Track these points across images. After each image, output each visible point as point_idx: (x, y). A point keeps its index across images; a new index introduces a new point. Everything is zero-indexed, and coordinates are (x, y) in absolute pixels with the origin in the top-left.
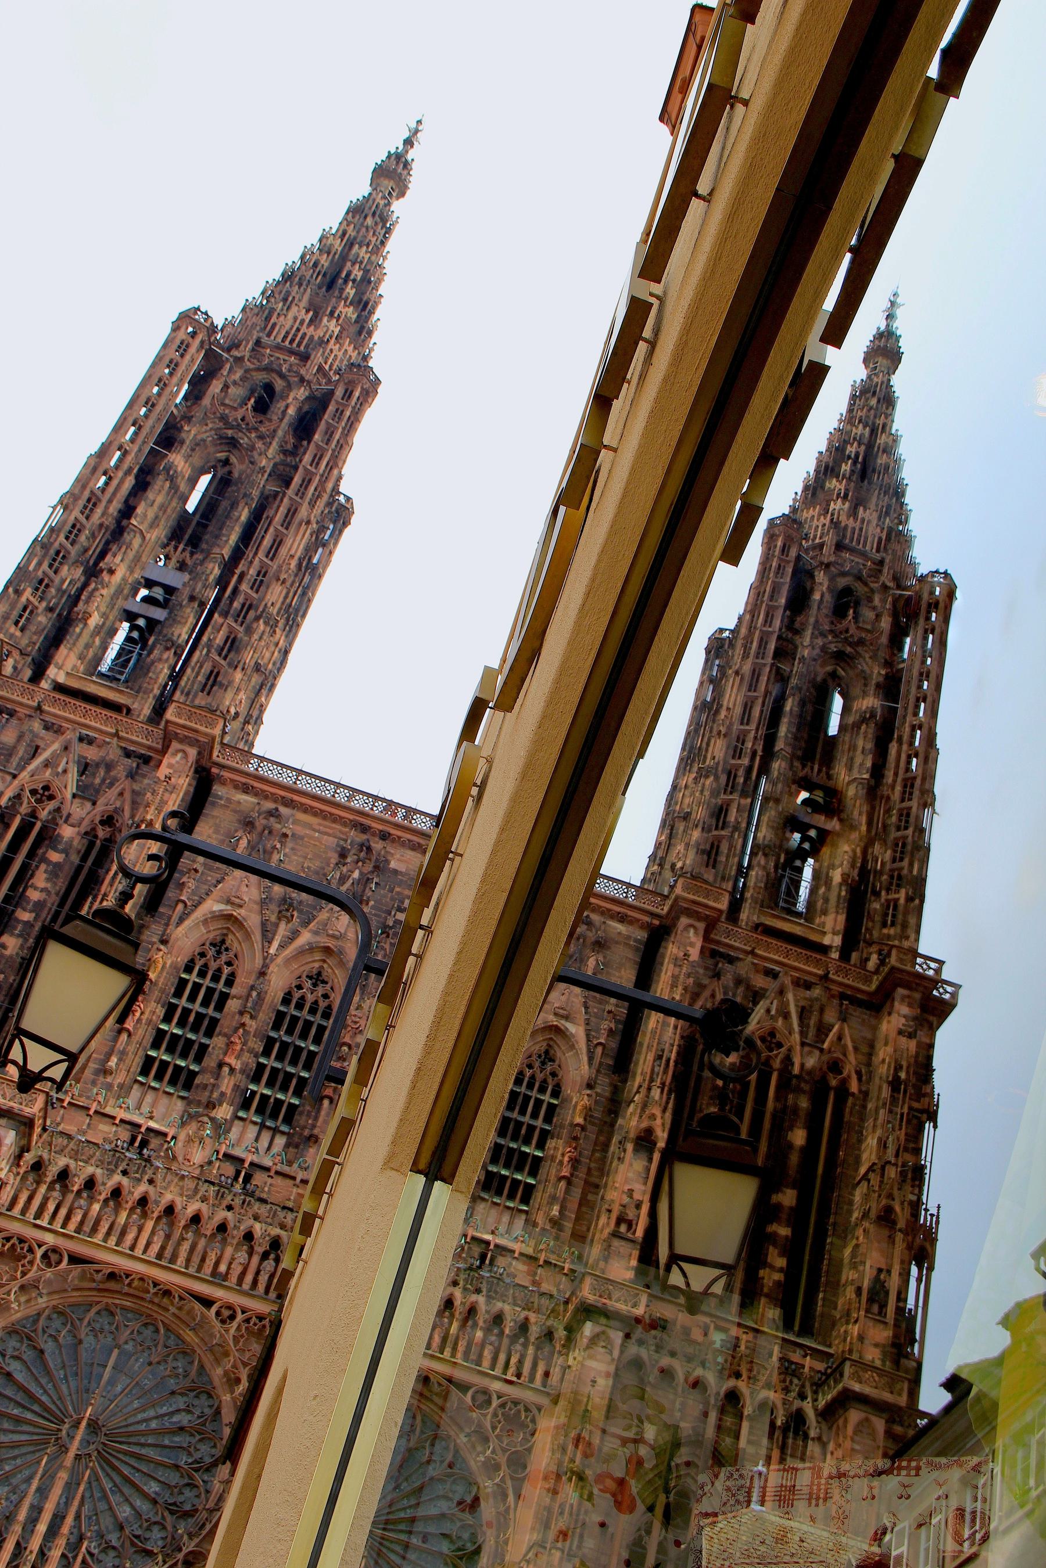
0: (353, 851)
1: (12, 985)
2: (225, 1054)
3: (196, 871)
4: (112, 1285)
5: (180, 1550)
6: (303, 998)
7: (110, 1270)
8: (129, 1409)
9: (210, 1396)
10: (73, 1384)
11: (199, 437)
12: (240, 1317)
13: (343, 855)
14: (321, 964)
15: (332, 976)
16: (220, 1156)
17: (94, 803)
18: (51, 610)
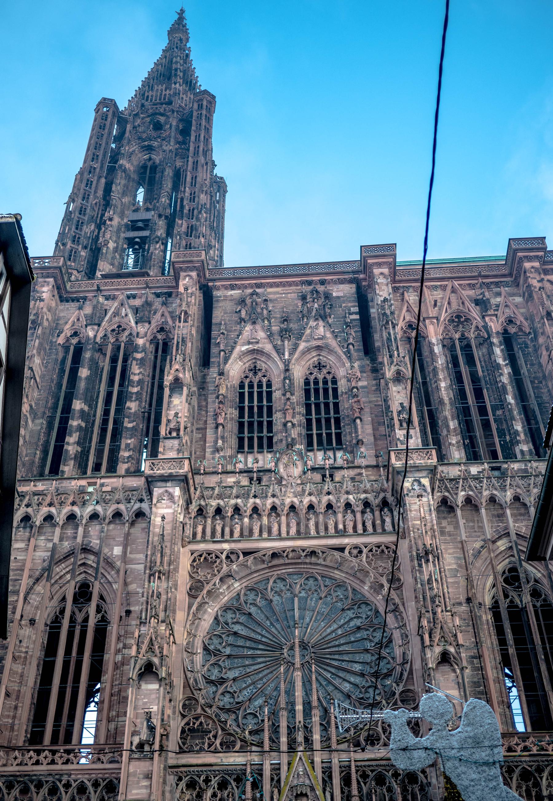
0: (308, 297)
1: (142, 429)
2: (285, 418)
3: (223, 333)
4: (276, 562)
5: (394, 694)
6: (316, 378)
7: (271, 552)
8: (320, 628)
9: (367, 604)
10: (278, 626)
11: (131, 150)
12: (365, 550)
13: (304, 298)
14: (318, 357)
15: (328, 361)
16: (309, 467)
17: (150, 323)
18: (86, 248)
